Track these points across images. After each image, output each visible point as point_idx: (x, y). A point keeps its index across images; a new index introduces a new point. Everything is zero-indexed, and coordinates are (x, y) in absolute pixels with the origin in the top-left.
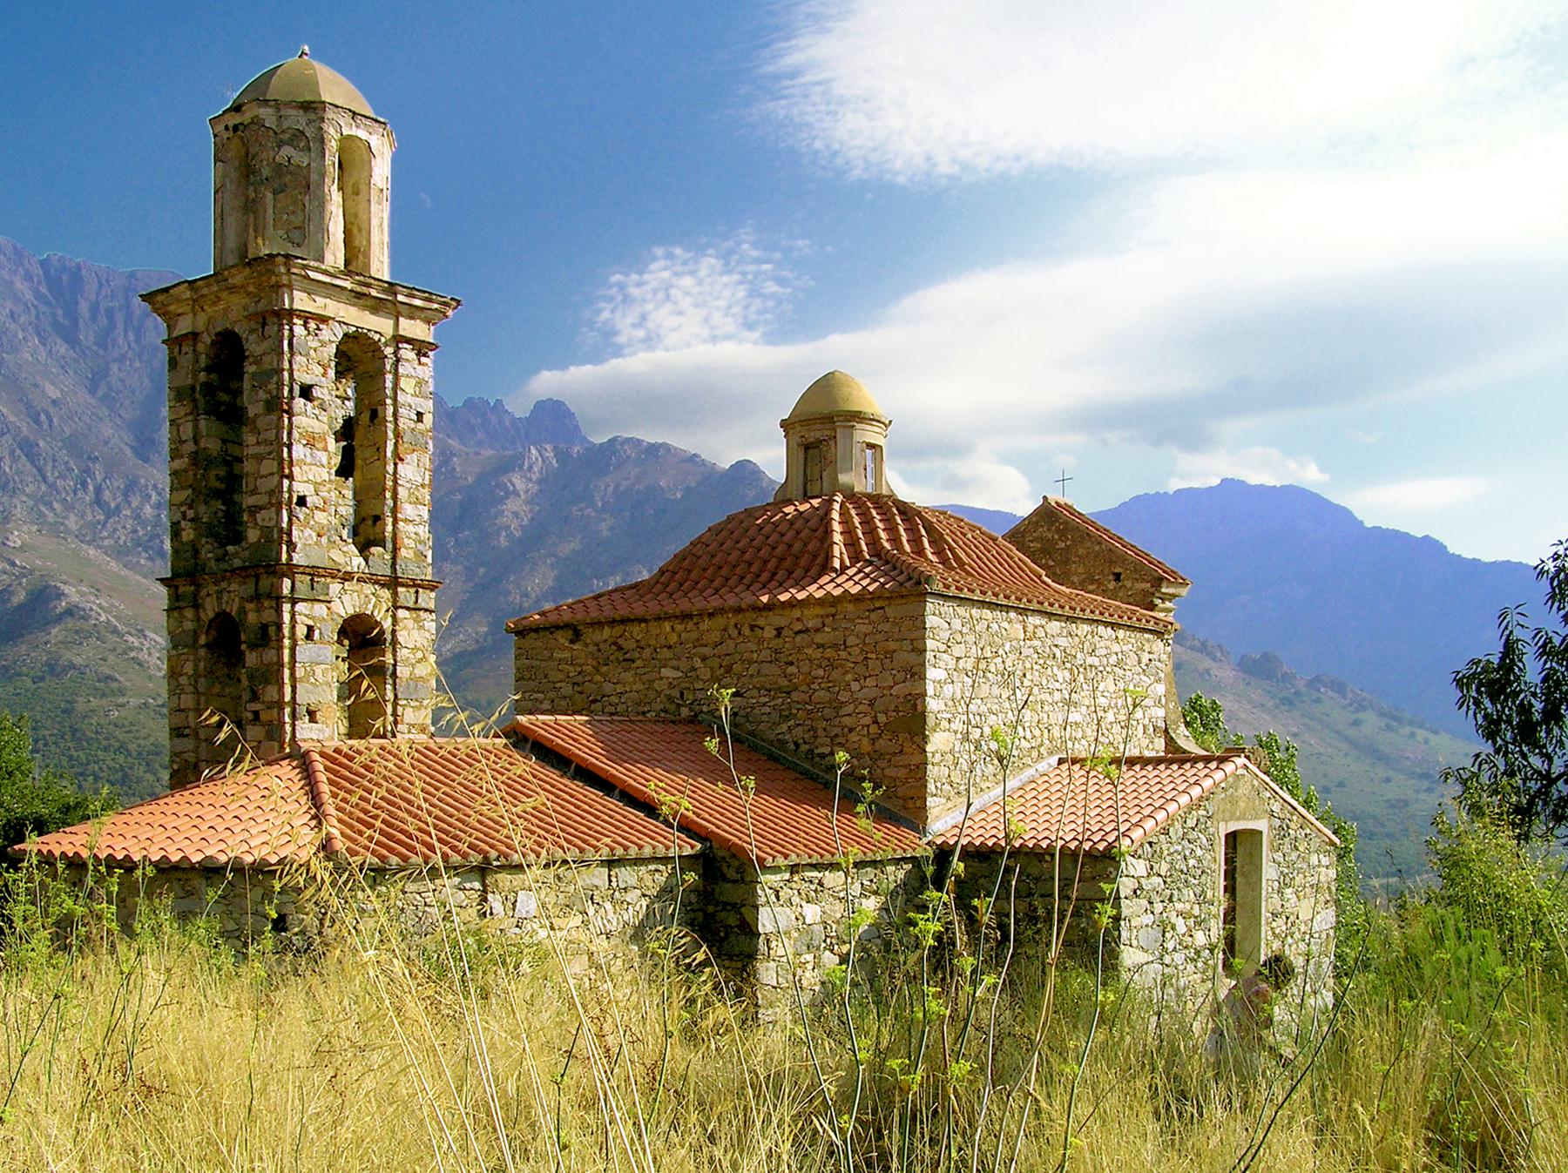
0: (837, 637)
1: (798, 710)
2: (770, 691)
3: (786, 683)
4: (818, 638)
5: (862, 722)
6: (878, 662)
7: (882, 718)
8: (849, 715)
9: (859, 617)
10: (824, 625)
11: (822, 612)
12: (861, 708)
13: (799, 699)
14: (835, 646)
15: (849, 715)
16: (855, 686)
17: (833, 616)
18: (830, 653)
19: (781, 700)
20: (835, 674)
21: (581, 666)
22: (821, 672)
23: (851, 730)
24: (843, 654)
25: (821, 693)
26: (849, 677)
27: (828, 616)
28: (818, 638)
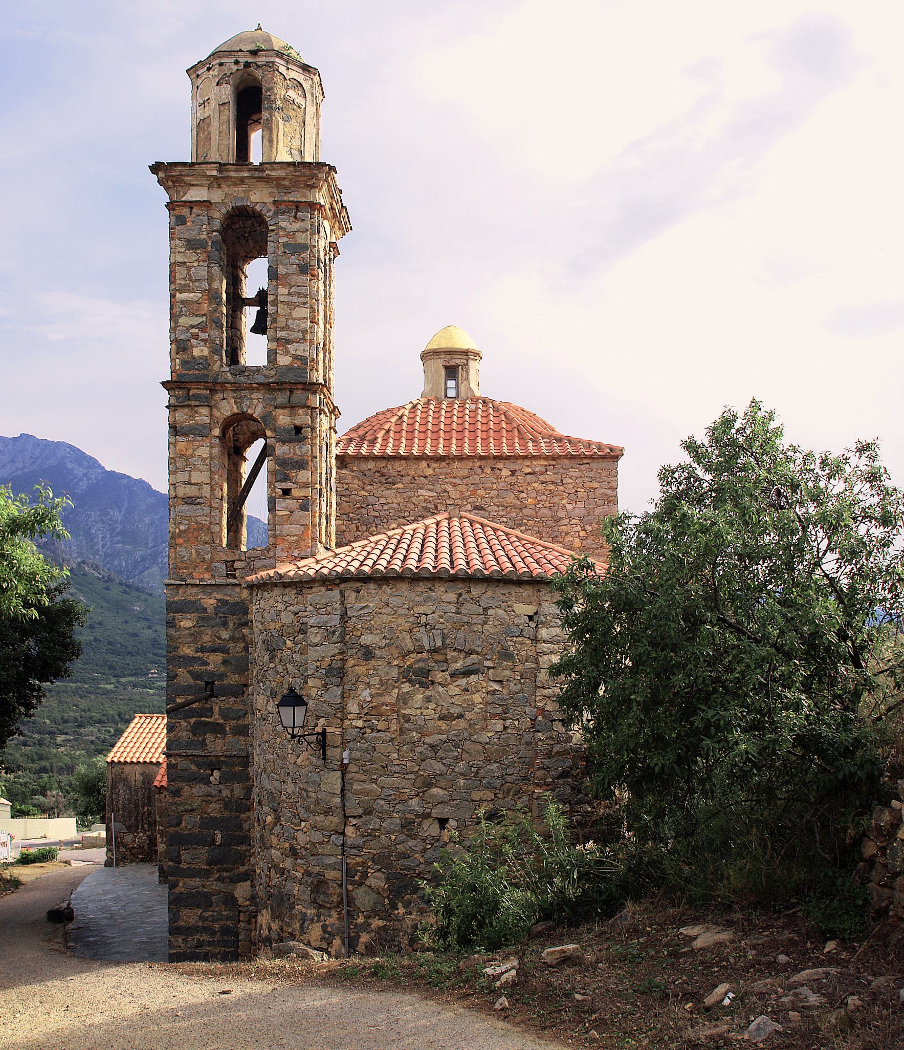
0: (557, 478)
1: (528, 520)
2: (507, 507)
3: (519, 503)
4: (542, 478)
5: (574, 529)
6: (585, 494)
7: (589, 528)
8: (566, 525)
9: (572, 468)
10: (547, 471)
11: (546, 463)
12: (574, 521)
13: (529, 514)
14: (553, 483)
15: (566, 525)
16: (569, 507)
17: (554, 466)
18: (552, 487)
19: (515, 514)
20: (556, 499)
21: (348, 484)
22: (544, 497)
23: (567, 534)
24: (561, 488)
25: (545, 511)
26: (564, 502)
27: (550, 465)
28: (542, 478)
